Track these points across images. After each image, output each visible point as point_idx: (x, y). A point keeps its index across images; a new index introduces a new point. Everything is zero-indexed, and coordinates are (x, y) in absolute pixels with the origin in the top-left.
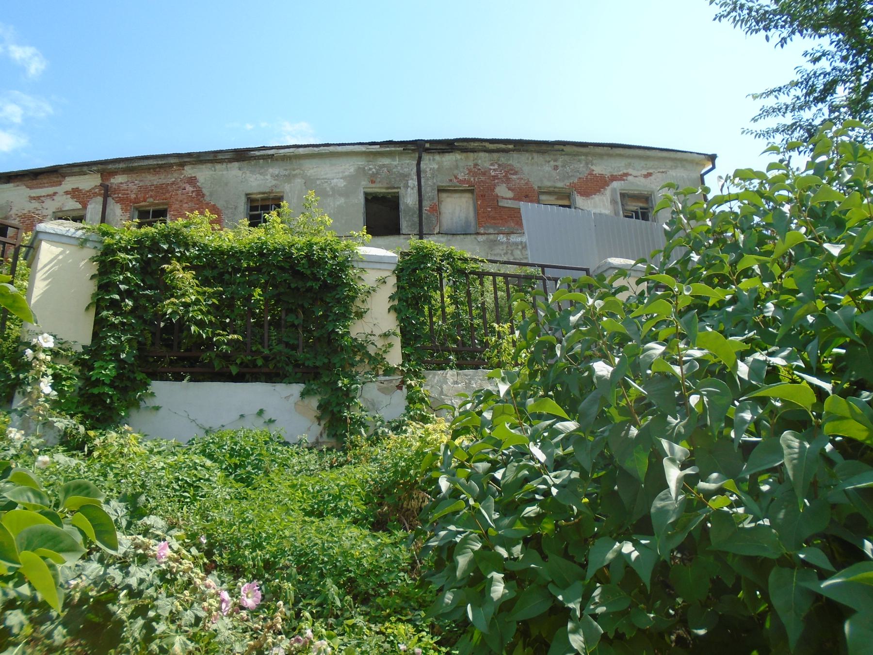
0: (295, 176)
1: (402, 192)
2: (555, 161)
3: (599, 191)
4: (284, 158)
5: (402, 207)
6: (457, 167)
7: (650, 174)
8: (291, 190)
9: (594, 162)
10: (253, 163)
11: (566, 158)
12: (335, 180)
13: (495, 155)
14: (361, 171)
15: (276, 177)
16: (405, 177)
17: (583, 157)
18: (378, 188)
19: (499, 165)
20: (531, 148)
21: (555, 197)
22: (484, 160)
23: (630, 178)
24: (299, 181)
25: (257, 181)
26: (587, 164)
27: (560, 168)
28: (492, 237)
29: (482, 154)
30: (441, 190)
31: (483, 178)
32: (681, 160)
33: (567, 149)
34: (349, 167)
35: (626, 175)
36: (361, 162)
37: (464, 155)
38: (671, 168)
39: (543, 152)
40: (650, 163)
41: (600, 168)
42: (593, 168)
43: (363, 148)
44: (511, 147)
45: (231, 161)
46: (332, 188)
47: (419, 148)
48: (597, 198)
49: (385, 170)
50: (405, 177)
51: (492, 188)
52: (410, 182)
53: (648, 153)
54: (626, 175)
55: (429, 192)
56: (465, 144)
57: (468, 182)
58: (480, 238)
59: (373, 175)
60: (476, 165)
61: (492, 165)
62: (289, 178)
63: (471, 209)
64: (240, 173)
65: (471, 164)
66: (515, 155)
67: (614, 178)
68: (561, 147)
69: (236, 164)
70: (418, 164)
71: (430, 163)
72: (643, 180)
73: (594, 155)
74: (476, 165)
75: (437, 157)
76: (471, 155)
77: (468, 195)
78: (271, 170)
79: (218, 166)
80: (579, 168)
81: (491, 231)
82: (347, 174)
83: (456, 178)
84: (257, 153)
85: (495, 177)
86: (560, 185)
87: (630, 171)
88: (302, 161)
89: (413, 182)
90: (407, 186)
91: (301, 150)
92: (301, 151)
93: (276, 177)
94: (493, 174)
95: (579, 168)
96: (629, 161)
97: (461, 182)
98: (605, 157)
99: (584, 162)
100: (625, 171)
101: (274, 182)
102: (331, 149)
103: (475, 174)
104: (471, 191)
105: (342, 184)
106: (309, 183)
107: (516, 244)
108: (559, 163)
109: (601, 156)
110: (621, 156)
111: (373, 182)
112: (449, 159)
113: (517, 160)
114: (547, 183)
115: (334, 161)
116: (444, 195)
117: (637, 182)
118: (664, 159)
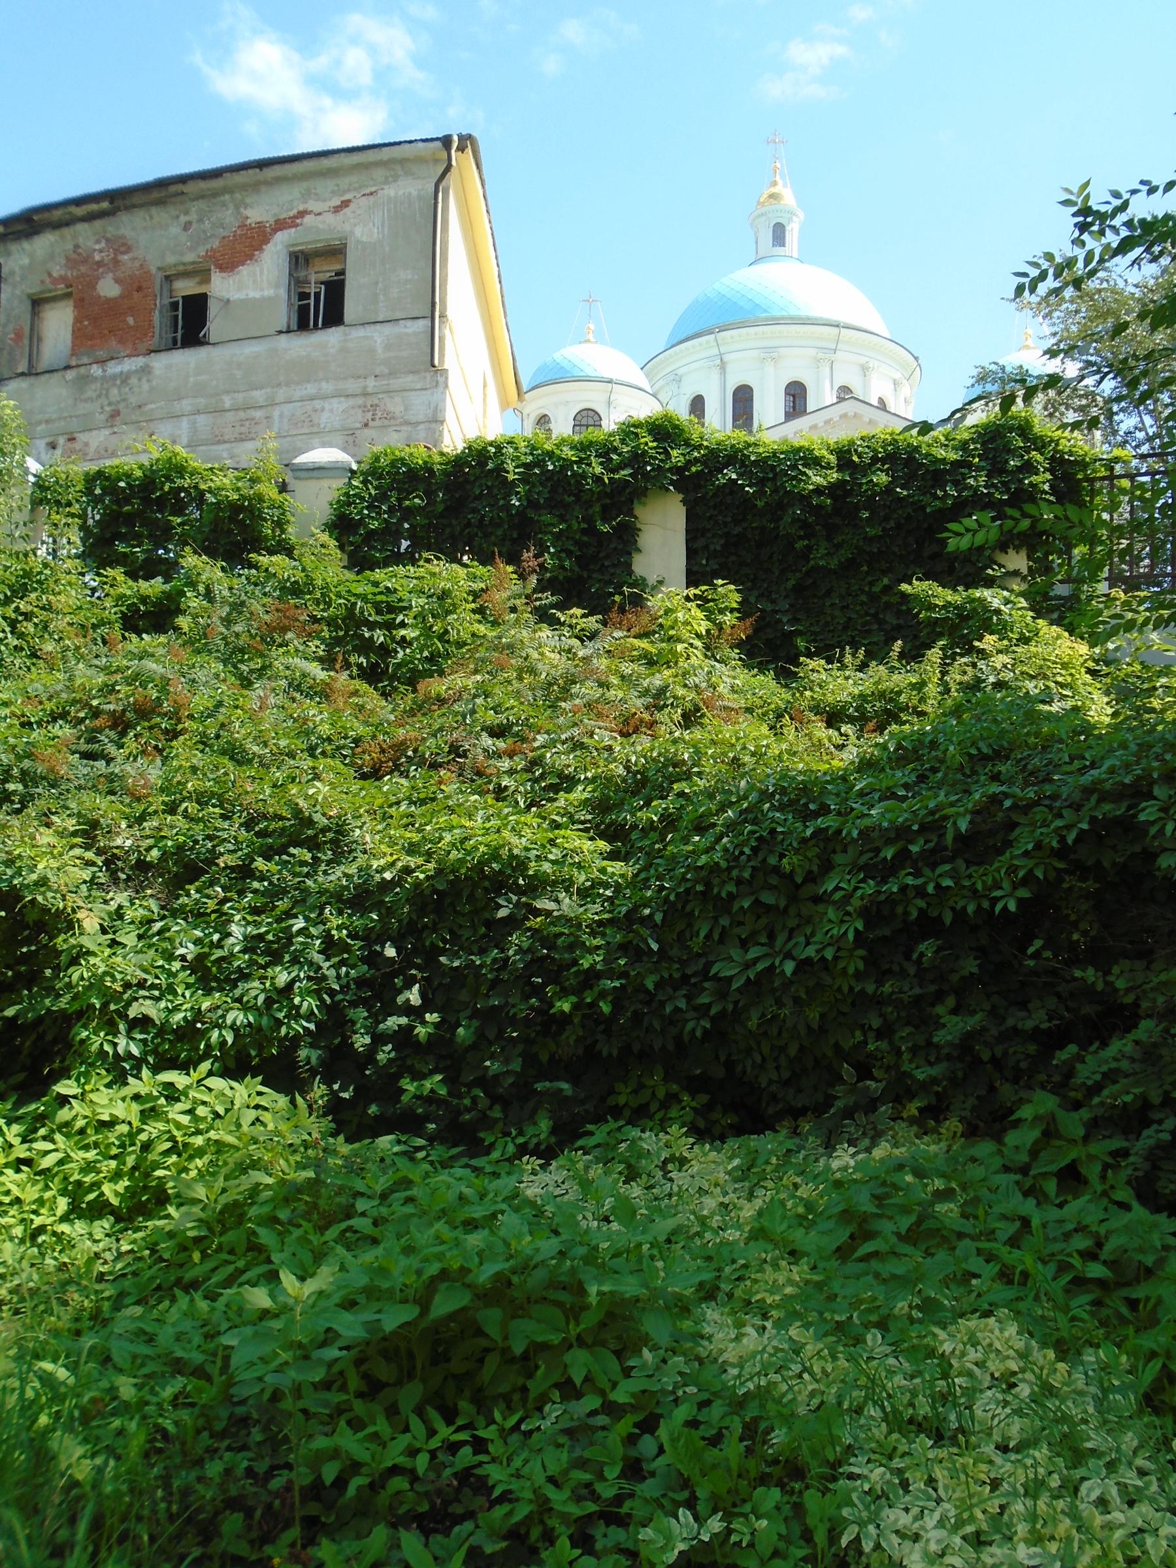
2: (187, 213)
3: (251, 257)
7: (346, 204)
9: (248, 200)
11: (201, 204)
13: (98, 224)
17: (227, 197)
19: (108, 240)
20: (137, 199)
21: (197, 279)
22: (86, 236)
23: (308, 219)
26: (237, 207)
27: (194, 226)
28: (82, 370)
29: (80, 227)
31: (83, 269)
32: (403, 161)
33: (190, 188)
35: (302, 214)
37: (57, 232)
38: (386, 182)
39: (161, 202)
40: (344, 182)
41: (260, 210)
42: (248, 212)
44: (105, 205)
48: (244, 271)
51: (93, 285)
53: (325, 163)
54: (302, 214)
56: (46, 215)
58: (70, 375)
60: (77, 246)
61: (98, 242)
65: (69, 246)
66: (124, 217)
67: (281, 225)
68: (179, 187)
72: (330, 218)
73: (244, 187)
74: (77, 246)
75: (26, 245)
76: (67, 232)
80: (225, 219)
81: (85, 360)
83: (50, 275)
85: (100, 264)
86: (190, 257)
87: (312, 205)
94: (97, 257)
95: (225, 219)
96: (305, 184)
97: (55, 281)
98: (263, 188)
99: (231, 206)
100: (301, 208)
107: (114, 377)
108: (193, 217)
109: (256, 187)
110: (279, 180)
112: (43, 243)
113: (129, 225)
114: (171, 259)
117: (321, 226)
118: (366, 166)
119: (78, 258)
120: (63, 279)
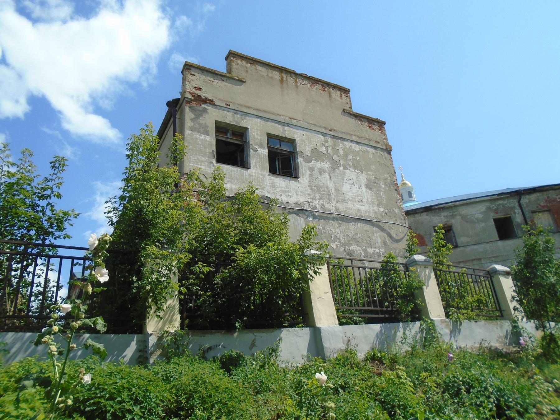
0: (456, 215)
1: (513, 216)
4: (451, 207)
5: (514, 223)
6: (538, 200)
8: (456, 223)
10: (433, 212)
12: (477, 215)
14: (489, 209)
15: (446, 217)
16: (513, 208)
18: (500, 216)
24: (458, 217)
25: (439, 220)
29: (551, 192)
30: (533, 212)
31: (554, 203)
34: (482, 207)
36: (488, 204)
43: (489, 198)
45: (422, 212)
46: (477, 219)
47: (519, 194)
49: (501, 206)
50: (513, 208)
52: (516, 211)
55: (527, 214)
57: (547, 206)
59: (495, 210)
61: (557, 196)
62: (453, 216)
63: (550, 219)
64: (427, 217)
65: (545, 197)
69: (425, 213)
70: (519, 202)
71: (525, 200)
74: (548, 197)
75: (527, 197)
76: (545, 193)
77: (546, 213)
78: (443, 214)
79: (416, 215)
82: (482, 211)
83: (540, 205)
84: (436, 207)
88: (458, 208)
89: (518, 210)
90: (515, 213)
91: (458, 203)
92: (458, 203)
93: (446, 217)
101: (446, 220)
102: (473, 200)
103: (549, 202)
104: (549, 211)
105: (480, 216)
106: (464, 217)
111: (497, 213)
112: (533, 197)
115: (474, 205)
116: (534, 214)
119: (549, 200)
120: (543, 207)
